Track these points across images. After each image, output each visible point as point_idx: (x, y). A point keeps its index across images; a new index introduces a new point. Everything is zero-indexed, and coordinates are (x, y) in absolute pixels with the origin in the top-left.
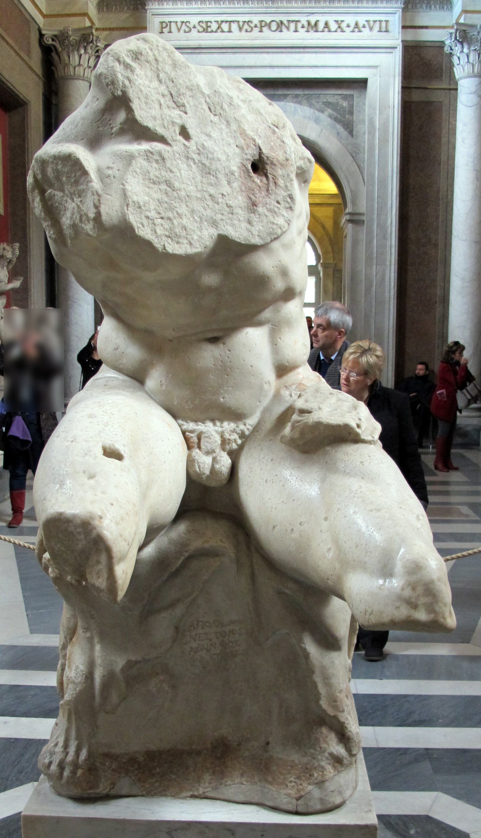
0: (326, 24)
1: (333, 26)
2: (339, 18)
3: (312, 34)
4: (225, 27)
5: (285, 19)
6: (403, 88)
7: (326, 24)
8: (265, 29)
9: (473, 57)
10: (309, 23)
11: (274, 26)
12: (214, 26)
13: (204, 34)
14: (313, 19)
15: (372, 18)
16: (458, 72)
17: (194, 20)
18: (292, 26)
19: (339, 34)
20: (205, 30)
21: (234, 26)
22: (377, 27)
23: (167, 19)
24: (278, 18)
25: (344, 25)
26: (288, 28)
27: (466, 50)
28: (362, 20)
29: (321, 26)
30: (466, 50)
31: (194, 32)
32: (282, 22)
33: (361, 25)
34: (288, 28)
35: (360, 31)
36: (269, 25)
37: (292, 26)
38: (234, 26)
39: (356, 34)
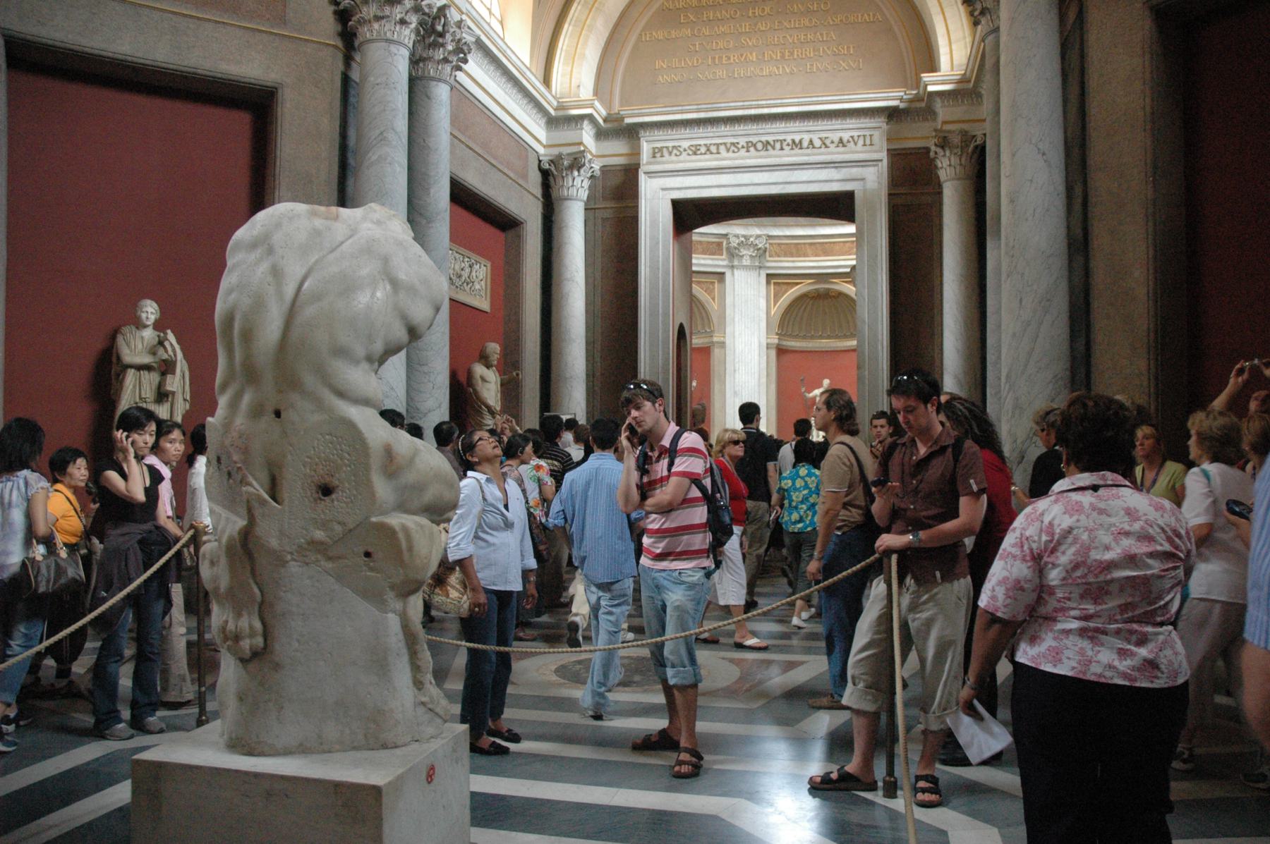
0: (811, 142)
1: (817, 143)
2: (823, 135)
3: (797, 151)
4: (713, 149)
5: (770, 138)
6: (890, 195)
7: (811, 142)
8: (752, 149)
9: (955, 160)
10: (793, 141)
11: (760, 146)
12: (703, 150)
13: (694, 157)
14: (797, 138)
15: (855, 134)
16: (942, 174)
17: (685, 144)
18: (778, 146)
19: (823, 150)
20: (695, 153)
21: (722, 148)
22: (861, 142)
23: (659, 145)
24: (764, 139)
25: (828, 142)
26: (774, 148)
27: (948, 153)
28: (846, 136)
29: (805, 144)
30: (948, 153)
31: (684, 154)
32: (768, 142)
33: (845, 140)
34: (774, 148)
35: (844, 146)
36: (754, 146)
37: (778, 146)
38: (722, 148)
39: (841, 149)
